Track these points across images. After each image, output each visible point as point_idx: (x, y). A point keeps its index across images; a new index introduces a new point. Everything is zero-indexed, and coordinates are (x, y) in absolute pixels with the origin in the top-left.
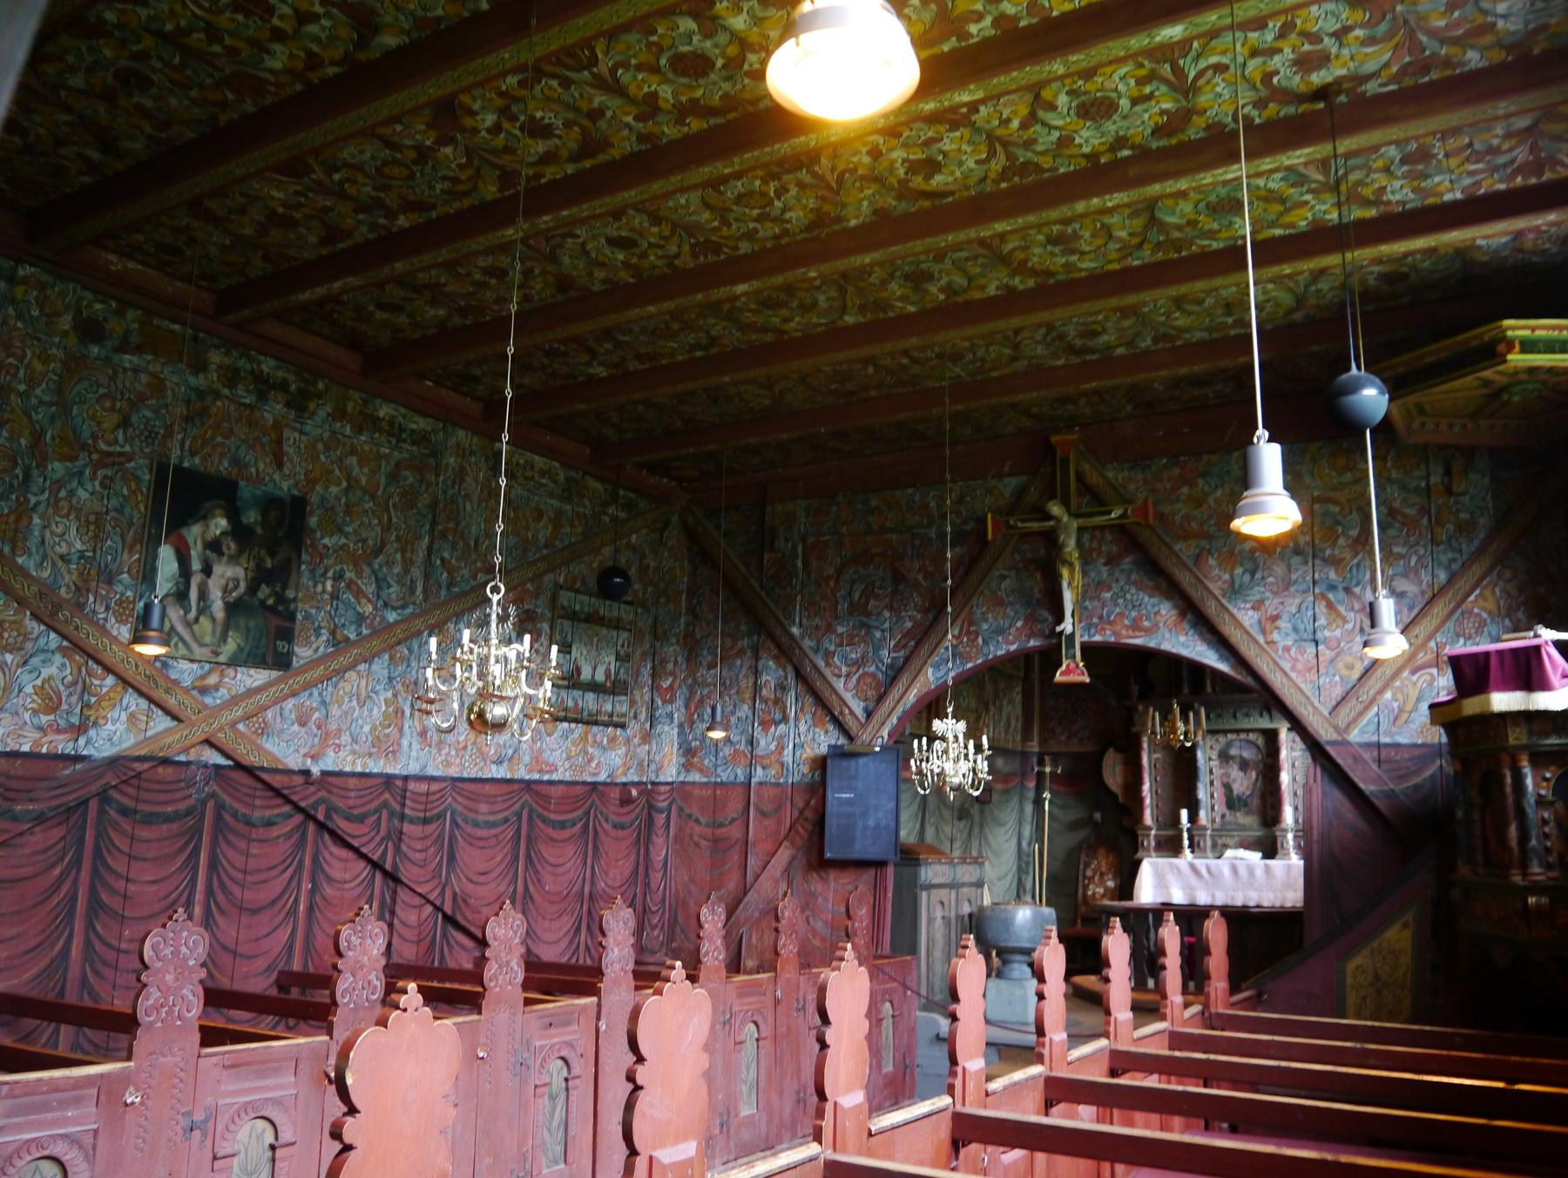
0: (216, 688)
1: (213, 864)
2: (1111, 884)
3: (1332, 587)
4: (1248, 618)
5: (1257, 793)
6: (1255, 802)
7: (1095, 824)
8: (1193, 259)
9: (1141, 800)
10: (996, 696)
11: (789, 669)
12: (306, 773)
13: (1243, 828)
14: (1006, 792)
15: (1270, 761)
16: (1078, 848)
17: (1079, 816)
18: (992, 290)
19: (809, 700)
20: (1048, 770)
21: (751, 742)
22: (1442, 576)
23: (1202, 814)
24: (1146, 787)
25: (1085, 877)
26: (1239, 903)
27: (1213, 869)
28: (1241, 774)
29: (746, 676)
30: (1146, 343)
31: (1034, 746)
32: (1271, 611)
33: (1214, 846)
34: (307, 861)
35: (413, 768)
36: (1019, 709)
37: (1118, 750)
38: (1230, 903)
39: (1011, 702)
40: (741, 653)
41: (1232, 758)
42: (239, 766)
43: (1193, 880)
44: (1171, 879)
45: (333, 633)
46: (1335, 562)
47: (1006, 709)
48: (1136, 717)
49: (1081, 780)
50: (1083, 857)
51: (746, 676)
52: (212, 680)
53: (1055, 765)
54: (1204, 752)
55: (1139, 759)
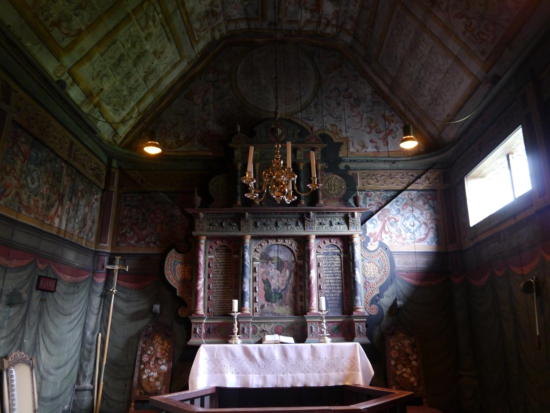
2: (164, 368)
5: (290, 288)
6: (288, 295)
7: (155, 314)
9: (197, 293)
10: (74, 192)
13: (278, 316)
14: (75, 284)
15: (301, 262)
16: (138, 336)
17: (141, 308)
20: (117, 267)
23: (247, 304)
24: (201, 282)
25: (141, 362)
26: (288, 385)
27: (265, 352)
28: (278, 272)
31: (107, 247)
33: (254, 332)
36: (96, 214)
37: (178, 251)
38: (280, 385)
39: (89, 204)
41: (271, 259)
43: (246, 364)
44: (226, 363)
47: (83, 210)
48: (197, 223)
49: (146, 276)
50: (141, 343)
53: (123, 263)
54: (250, 254)
55: (197, 257)
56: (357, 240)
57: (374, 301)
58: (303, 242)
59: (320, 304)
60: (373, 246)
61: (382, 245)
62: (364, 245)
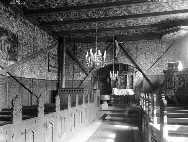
0: (7, 64)
1: (9, 91)
3: (148, 58)
4: (138, 61)
6: (124, 83)
8: (149, 14)
11: (79, 65)
12: (21, 78)
18: (123, 15)
19: (81, 70)
21: (73, 75)
22: (160, 57)
29: (72, 67)
30: (135, 25)
32: (140, 60)
34: (21, 91)
35: (33, 78)
40: (71, 64)
42: (12, 76)
45: (22, 56)
46: (148, 55)
51: (72, 67)
52: (7, 63)
56: (134, 75)
57: (136, 84)
58: (126, 76)
59: (128, 84)
60: (137, 76)
61: (138, 76)
62: (135, 76)
